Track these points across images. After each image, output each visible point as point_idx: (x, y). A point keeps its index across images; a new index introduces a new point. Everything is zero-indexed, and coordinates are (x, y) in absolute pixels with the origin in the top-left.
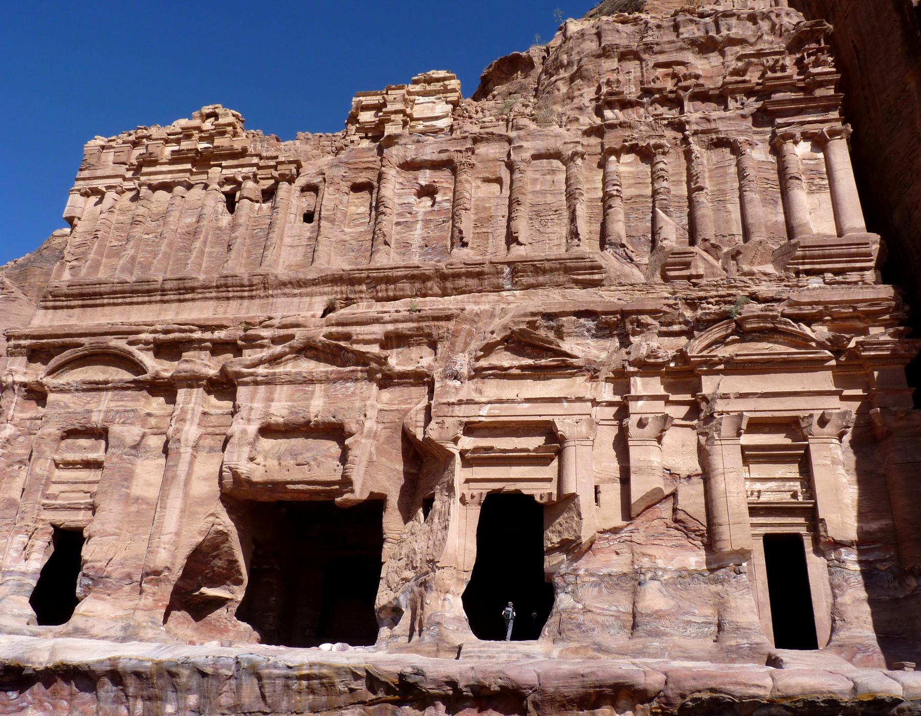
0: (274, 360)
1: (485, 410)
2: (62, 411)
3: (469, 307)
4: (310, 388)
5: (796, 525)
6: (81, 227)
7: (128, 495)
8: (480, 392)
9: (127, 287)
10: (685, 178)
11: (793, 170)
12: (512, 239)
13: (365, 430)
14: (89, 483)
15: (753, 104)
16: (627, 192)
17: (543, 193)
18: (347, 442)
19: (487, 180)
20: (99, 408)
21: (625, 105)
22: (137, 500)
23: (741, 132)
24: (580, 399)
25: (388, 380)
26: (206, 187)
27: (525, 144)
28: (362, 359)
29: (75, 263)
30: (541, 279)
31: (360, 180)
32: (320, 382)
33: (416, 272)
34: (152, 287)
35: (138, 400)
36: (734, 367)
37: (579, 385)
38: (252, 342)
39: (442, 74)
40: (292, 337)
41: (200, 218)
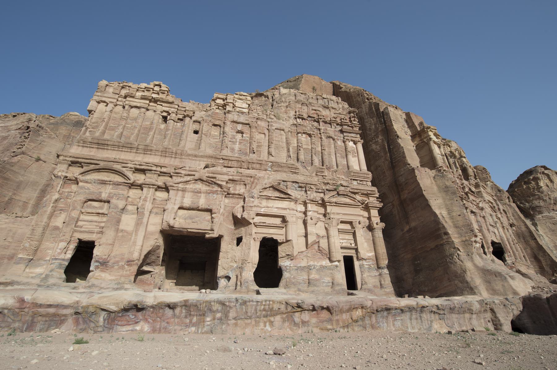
1: (263, 210)
2: (87, 191)
3: (258, 175)
4: (200, 195)
5: (352, 253)
6: (96, 115)
7: (118, 229)
8: (261, 204)
9: (121, 144)
10: (320, 145)
11: (349, 149)
12: (270, 154)
13: (221, 212)
14: (99, 222)
15: (339, 128)
16: (304, 146)
17: (279, 141)
18: (213, 216)
19: (260, 133)
20: (106, 192)
21: (303, 119)
22: (122, 231)
23: (335, 136)
24: (293, 210)
25: (228, 195)
26: (155, 111)
27: (274, 124)
28: (220, 186)
29: (92, 129)
30: (280, 169)
31: (216, 123)
32: (204, 193)
33: (240, 159)
34: (133, 146)
35: (124, 190)
36: (337, 204)
37: (292, 205)
39: (245, 94)
40: (194, 175)
41: (152, 123)
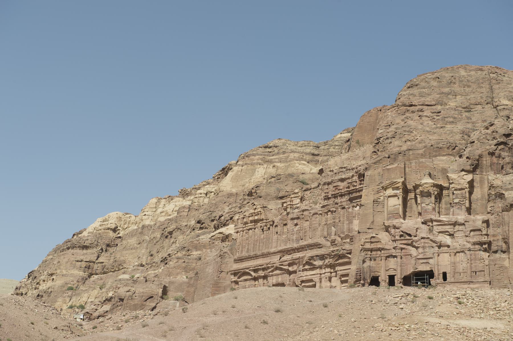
0: (272, 271)
1: (304, 278)
19: (306, 221)
25: (290, 273)
38: (268, 268)
